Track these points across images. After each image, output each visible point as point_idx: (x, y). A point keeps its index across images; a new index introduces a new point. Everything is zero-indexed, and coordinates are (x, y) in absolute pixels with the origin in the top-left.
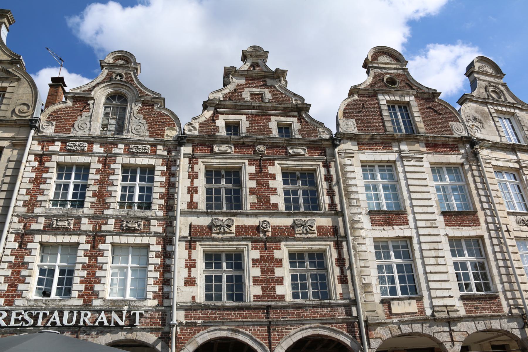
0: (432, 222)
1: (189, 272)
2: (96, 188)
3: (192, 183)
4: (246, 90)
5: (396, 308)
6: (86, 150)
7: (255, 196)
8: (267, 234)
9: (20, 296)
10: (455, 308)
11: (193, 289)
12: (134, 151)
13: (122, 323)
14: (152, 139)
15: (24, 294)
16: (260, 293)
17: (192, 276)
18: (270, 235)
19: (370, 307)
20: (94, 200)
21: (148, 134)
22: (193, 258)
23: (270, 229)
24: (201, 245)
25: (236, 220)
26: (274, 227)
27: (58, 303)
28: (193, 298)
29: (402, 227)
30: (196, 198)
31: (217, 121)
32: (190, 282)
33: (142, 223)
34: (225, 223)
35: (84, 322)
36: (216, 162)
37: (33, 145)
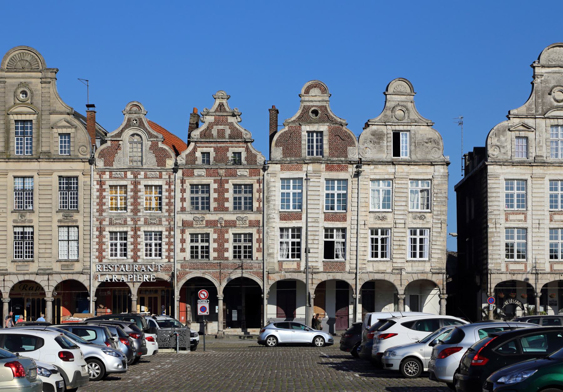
0: (316, 219)
1: (182, 245)
2: (132, 200)
3: (183, 196)
4: (215, 127)
5: (285, 266)
6: (123, 177)
7: (216, 203)
8: (222, 225)
9: (104, 258)
10: (318, 267)
11: (184, 253)
12: (150, 176)
13: (152, 270)
14: (159, 168)
15: (106, 257)
16: (217, 256)
17: (184, 247)
18: (223, 226)
19: (271, 265)
20: (132, 207)
21: (157, 164)
22: (184, 238)
23: (223, 223)
24: (188, 231)
25: (206, 217)
26: (225, 221)
27: (122, 261)
28: (185, 258)
29: (297, 221)
30: (185, 205)
31: (196, 152)
32: (183, 250)
33: (158, 220)
34: (200, 219)
35: (135, 270)
36: (195, 181)
37: (96, 176)
